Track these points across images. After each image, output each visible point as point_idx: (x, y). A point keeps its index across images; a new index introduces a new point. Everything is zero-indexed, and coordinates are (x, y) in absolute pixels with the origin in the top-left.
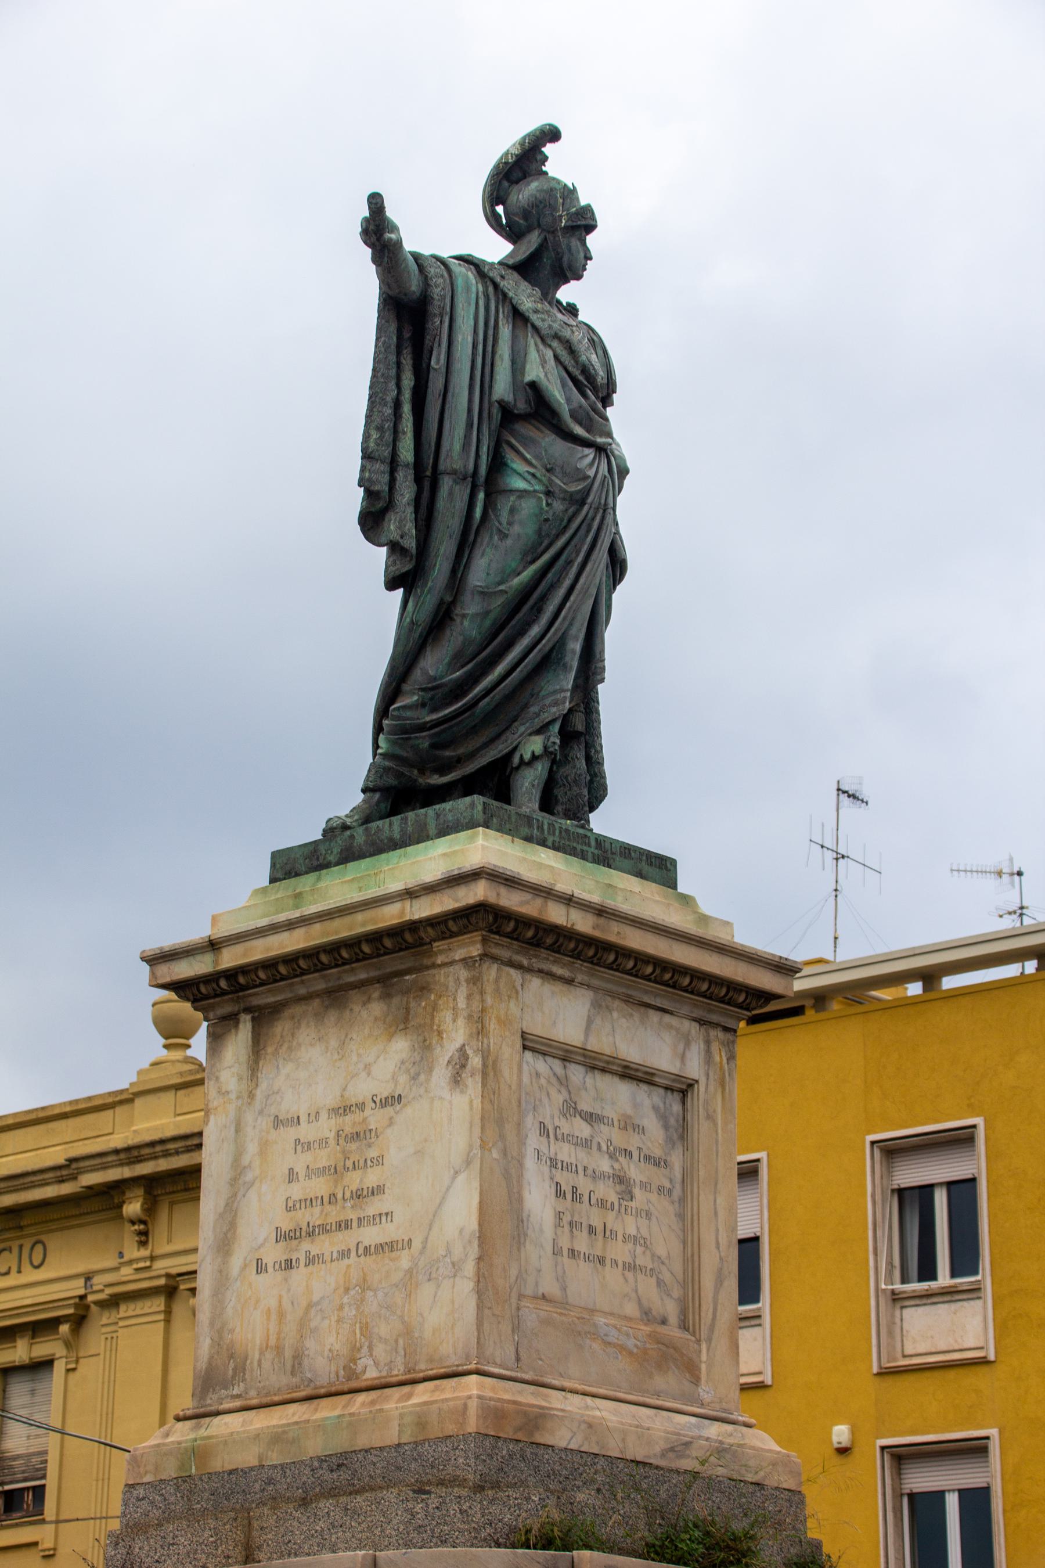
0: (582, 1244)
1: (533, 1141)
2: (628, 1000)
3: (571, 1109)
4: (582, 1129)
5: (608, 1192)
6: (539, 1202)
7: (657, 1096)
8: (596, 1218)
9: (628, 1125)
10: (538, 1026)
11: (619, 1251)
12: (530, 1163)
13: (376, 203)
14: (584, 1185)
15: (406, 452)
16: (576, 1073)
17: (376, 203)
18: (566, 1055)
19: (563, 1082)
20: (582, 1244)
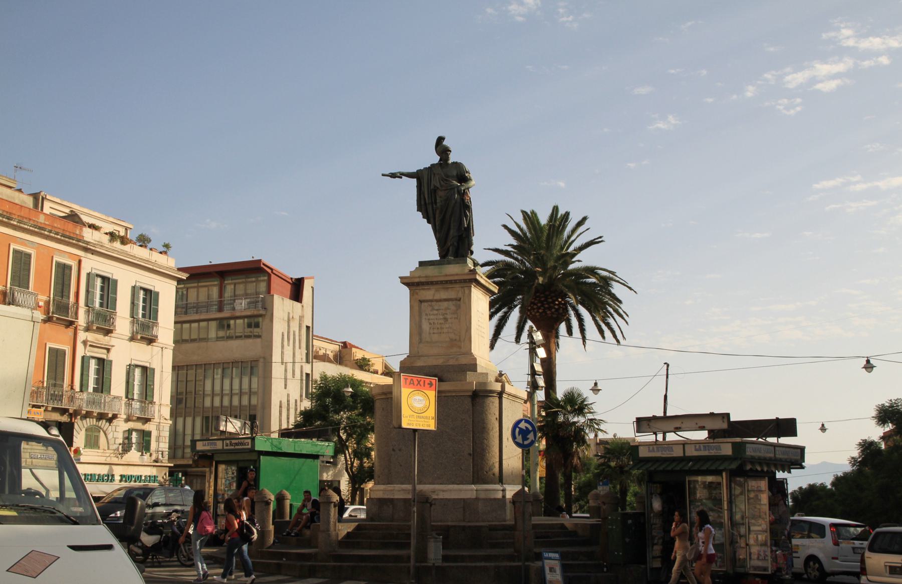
0: (436, 331)
1: (424, 317)
2: (444, 288)
3: (433, 309)
4: (435, 312)
5: (442, 321)
6: (426, 326)
7: (454, 302)
8: (439, 326)
9: (447, 309)
10: (423, 298)
11: (445, 330)
12: (423, 321)
13: (383, 175)
14: (436, 321)
15: (423, 203)
16: (433, 303)
17: (383, 175)
18: (431, 301)
19: (431, 306)
20: (436, 331)
